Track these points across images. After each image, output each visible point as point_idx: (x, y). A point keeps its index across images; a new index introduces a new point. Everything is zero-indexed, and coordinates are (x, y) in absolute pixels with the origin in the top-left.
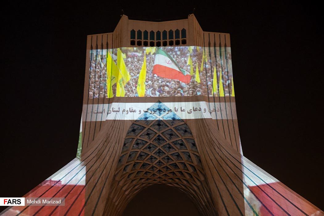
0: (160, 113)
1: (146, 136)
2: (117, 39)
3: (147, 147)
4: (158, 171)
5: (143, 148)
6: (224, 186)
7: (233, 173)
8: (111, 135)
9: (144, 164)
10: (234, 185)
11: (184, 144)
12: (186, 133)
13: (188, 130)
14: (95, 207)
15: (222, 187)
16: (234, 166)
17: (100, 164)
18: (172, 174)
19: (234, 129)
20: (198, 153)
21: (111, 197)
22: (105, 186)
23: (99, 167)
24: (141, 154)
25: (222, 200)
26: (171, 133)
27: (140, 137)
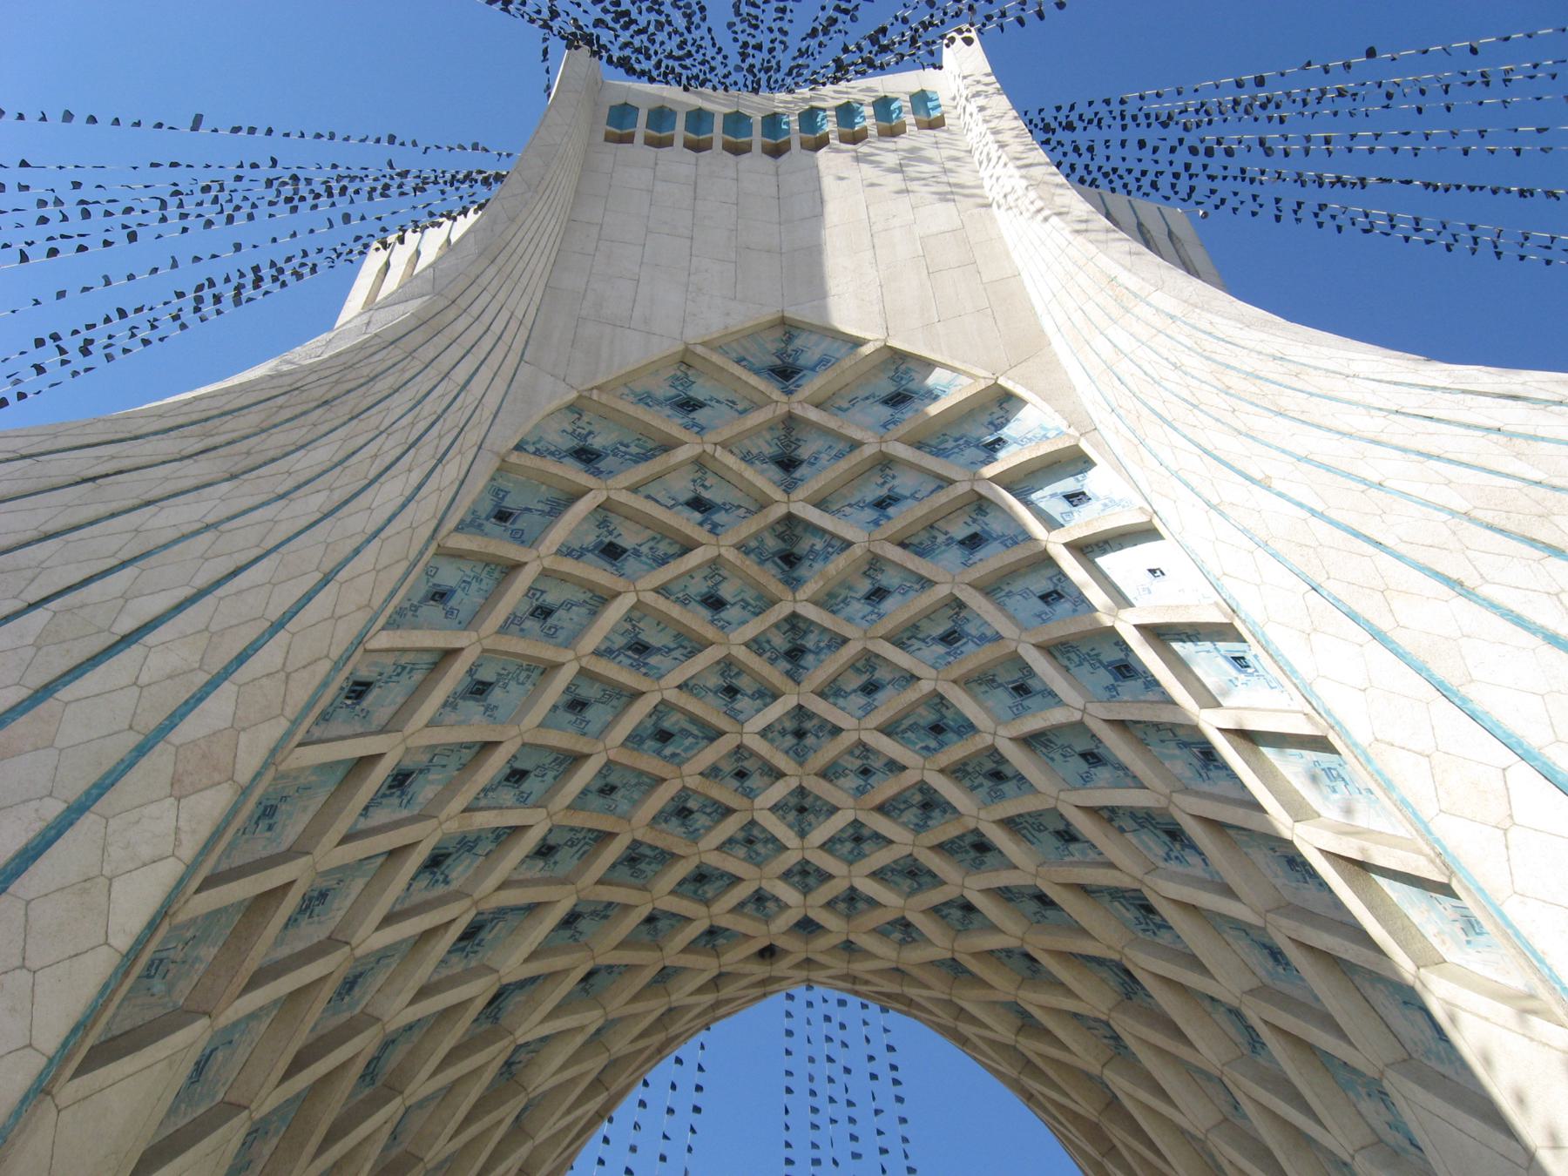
8: (382, 386)
24: (643, 637)
26: (884, 492)
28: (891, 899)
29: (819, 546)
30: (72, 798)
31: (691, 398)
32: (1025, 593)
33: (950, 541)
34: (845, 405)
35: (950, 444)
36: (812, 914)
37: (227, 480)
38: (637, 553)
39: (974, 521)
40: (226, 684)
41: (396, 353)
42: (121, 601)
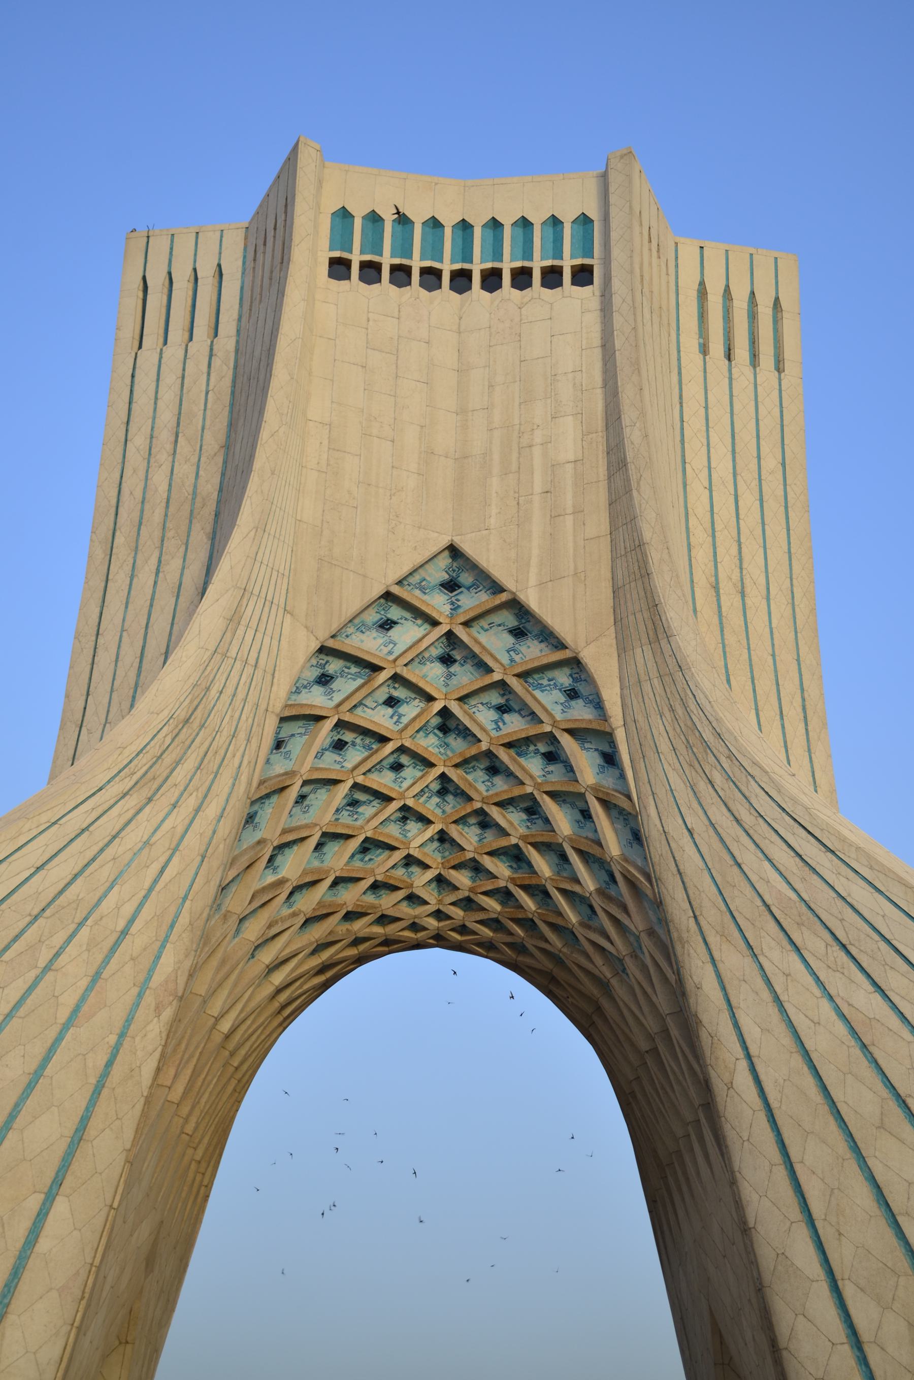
0: (452, 603)
1: (382, 712)
2: (264, 253)
3: (385, 763)
4: (430, 881)
5: (364, 769)
6: (748, 960)
7: (793, 896)
8: (214, 692)
9: (367, 845)
10: (794, 957)
11: (563, 757)
12: (573, 703)
13: (582, 688)
14: (122, 1035)
15: (733, 960)
16: (801, 864)
17: (156, 831)
18: (497, 896)
19: (804, 700)
20: (629, 797)
21: (201, 989)
22: (173, 938)
23: (147, 843)
25: (736, 1025)
27: (351, 710)
28: (487, 932)
29: (461, 727)
30: (118, 1031)
31: (388, 620)
32: (573, 805)
33: (537, 752)
34: (487, 627)
35: (545, 682)
36: (441, 933)
37: (147, 804)
38: (354, 744)
39: (552, 743)
40: (168, 945)
41: (218, 657)
42: (116, 910)
